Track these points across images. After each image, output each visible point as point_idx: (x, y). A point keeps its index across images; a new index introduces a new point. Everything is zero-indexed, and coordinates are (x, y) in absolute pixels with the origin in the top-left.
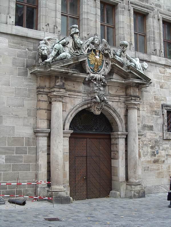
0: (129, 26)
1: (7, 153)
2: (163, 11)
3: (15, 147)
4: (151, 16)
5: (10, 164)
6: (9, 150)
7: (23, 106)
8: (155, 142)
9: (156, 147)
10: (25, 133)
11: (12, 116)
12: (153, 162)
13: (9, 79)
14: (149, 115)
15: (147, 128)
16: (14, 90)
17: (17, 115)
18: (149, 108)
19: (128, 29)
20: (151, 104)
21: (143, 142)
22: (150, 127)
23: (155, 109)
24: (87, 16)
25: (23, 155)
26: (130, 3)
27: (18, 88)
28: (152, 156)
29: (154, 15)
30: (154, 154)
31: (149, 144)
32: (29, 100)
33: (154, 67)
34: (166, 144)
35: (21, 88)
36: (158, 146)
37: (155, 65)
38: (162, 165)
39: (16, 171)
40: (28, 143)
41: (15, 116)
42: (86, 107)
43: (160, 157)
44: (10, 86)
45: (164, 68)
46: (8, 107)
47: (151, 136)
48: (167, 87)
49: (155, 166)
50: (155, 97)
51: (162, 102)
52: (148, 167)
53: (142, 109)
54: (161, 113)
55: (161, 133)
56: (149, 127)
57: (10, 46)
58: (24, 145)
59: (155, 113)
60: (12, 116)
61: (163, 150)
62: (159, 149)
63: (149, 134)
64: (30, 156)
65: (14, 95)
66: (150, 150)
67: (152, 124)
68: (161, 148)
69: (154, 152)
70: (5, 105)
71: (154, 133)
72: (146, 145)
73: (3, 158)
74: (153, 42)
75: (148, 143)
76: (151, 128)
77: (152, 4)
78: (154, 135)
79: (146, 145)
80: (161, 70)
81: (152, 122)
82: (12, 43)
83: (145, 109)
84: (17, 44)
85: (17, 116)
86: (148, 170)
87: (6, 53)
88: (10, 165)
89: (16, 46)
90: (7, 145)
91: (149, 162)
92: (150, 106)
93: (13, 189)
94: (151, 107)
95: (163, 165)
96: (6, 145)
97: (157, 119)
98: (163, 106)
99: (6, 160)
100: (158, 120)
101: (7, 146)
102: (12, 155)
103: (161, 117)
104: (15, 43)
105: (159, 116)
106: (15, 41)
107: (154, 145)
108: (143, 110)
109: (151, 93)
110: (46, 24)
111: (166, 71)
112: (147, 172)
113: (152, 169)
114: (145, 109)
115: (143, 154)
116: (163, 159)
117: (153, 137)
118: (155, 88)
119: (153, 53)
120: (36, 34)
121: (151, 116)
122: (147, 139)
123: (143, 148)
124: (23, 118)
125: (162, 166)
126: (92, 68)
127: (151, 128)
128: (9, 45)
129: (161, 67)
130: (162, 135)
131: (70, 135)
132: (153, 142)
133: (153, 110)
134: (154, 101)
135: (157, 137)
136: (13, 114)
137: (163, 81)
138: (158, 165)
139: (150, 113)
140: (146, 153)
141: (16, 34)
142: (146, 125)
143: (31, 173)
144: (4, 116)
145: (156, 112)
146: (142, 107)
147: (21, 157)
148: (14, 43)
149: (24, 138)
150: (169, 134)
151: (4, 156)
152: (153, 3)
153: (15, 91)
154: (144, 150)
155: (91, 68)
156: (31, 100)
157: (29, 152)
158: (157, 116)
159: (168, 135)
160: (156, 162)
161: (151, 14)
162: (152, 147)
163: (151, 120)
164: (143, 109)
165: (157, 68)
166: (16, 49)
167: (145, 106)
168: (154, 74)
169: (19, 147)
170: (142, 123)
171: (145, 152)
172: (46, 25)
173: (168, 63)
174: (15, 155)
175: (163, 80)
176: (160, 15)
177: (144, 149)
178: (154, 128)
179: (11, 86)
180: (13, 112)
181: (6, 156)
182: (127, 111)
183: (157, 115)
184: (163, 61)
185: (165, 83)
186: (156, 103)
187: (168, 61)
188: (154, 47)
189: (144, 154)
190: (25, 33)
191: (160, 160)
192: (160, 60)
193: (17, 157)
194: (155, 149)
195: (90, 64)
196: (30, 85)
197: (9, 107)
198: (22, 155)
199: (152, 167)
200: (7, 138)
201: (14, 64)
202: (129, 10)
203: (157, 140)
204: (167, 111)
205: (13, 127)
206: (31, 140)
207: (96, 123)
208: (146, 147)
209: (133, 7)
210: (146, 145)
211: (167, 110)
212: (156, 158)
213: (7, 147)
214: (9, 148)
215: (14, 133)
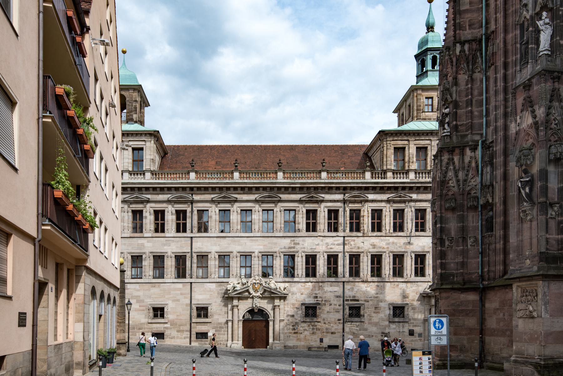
49: (295, 335)
66: (291, 327)
85: (220, 314)
91: (290, 333)
95: (301, 335)
109: (291, 299)
135: (297, 321)
160: (295, 333)
162: (293, 326)
176: (303, 254)
184: (304, 280)
201: (218, 294)
212: (296, 331)
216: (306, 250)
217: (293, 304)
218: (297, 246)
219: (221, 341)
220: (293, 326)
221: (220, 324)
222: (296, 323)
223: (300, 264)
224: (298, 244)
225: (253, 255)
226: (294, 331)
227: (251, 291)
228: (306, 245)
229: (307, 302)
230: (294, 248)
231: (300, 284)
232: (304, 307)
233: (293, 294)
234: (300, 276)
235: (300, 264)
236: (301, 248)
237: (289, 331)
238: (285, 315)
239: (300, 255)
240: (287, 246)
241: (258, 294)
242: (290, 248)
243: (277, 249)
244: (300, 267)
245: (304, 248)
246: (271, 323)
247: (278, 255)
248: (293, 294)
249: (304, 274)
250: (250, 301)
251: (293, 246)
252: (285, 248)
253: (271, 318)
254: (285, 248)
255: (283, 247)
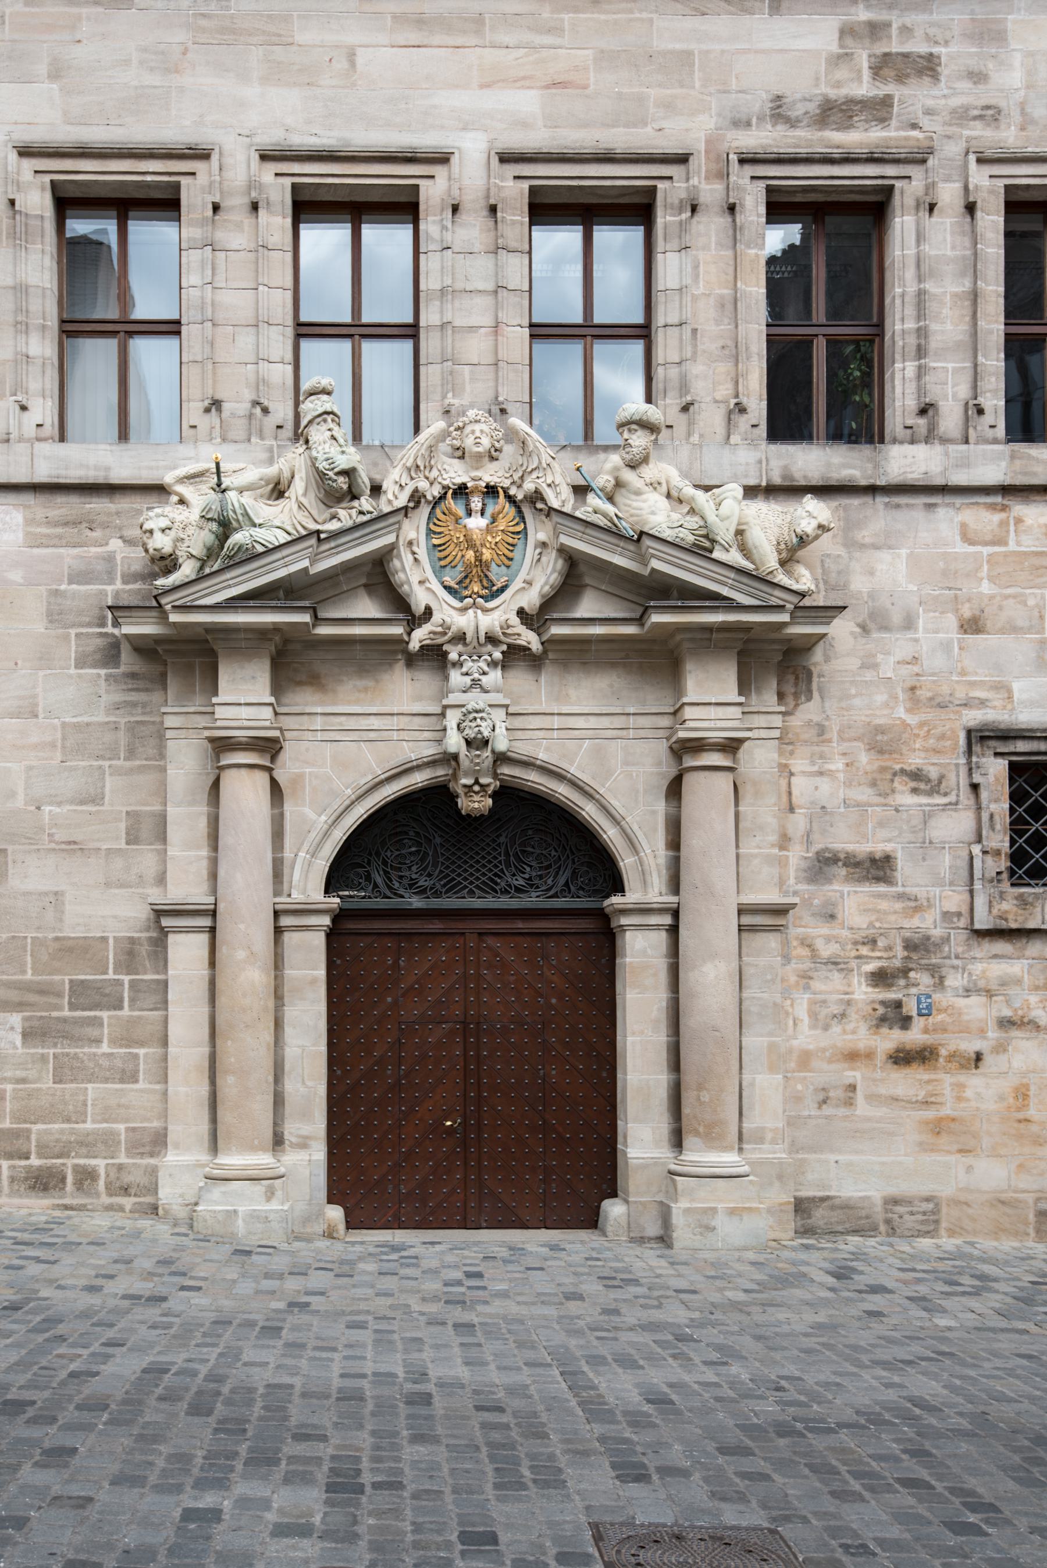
0: (729, 307)
1: (30, 1005)
2: (1019, 144)
3: (67, 978)
4: (909, 201)
5: (43, 1055)
6: (42, 992)
7: (97, 799)
8: (910, 946)
9: (912, 974)
10: (115, 917)
11: (53, 845)
12: (891, 1057)
13: (34, 687)
14: (864, 794)
15: (843, 872)
16: (59, 735)
17: (75, 843)
18: (864, 759)
19: (718, 323)
20: (880, 730)
21: (809, 946)
22: (867, 864)
23: (915, 761)
24: (442, 312)
25: (105, 1015)
26: (742, 161)
27: (77, 727)
28: (878, 1026)
29: (930, 187)
30: (895, 1016)
31: (858, 957)
32: (130, 771)
33: (919, 515)
34: (995, 956)
35: (88, 724)
36: (933, 970)
37: (921, 500)
38: (962, 1078)
39: (72, 1081)
40: (129, 958)
41: (63, 846)
42: (418, 779)
43: (945, 1030)
44: (36, 716)
45: (1004, 508)
46: (33, 808)
47: (878, 911)
48: (1020, 623)
49: (905, 1082)
50: (913, 689)
51: (974, 717)
52: (852, 1088)
53: (813, 763)
54: (964, 782)
55: (959, 893)
56: (857, 864)
57: (34, 542)
58: (111, 971)
59: (913, 784)
60: (53, 845)
61: (968, 992)
62: (940, 983)
63: (856, 903)
64: (140, 1017)
65: (59, 756)
66: (864, 993)
67: (888, 847)
68: (955, 981)
69: (898, 1005)
70: (20, 802)
71: (901, 896)
72: (836, 963)
73: (12, 1028)
74: (911, 368)
75: (854, 953)
76: (878, 868)
77: (925, 122)
78: (898, 906)
79: (834, 962)
80: (972, 525)
81: (883, 833)
82: (39, 525)
83: (838, 764)
84: (66, 524)
85: (73, 847)
86: (849, 1103)
87: (16, 576)
88: (44, 1058)
89: (60, 537)
90: (30, 972)
91: (852, 1057)
92: (878, 749)
93: (58, 1157)
94: (881, 752)
95: (975, 1082)
96: (24, 972)
97: (927, 818)
98: (980, 737)
99: (26, 1035)
100: (932, 823)
101: (29, 976)
102: (55, 1014)
103: (957, 804)
104: (56, 524)
105: (946, 794)
106: (56, 512)
107: (897, 963)
108: (821, 773)
109: (860, 677)
110: (206, 403)
111: (1019, 521)
112: (842, 1111)
113: (880, 1096)
114: (832, 767)
115: (813, 1015)
116: (969, 1046)
117: (893, 918)
118: (916, 640)
119: (909, 431)
120: (153, 464)
121: (882, 800)
122: (845, 933)
123: (811, 982)
124: (103, 853)
125: (961, 1086)
126: (453, 584)
127: (878, 868)
128: (27, 534)
129: (977, 503)
130: (965, 909)
131: (326, 921)
132: (889, 948)
133: (897, 767)
134: (909, 711)
135: (928, 923)
136: (57, 838)
137: (986, 588)
138: (926, 1077)
139: (873, 784)
140: (836, 1009)
141: (56, 480)
142: (842, 856)
143: (142, 1091)
144: (17, 847)
145: (916, 775)
146: (813, 755)
147: (97, 1022)
148: (49, 523)
149: (111, 941)
150: (1020, 897)
151: (16, 1019)
152: (929, 112)
153: (64, 738)
154: (820, 993)
155: (445, 587)
156: (141, 769)
157: (132, 1000)
158: (924, 800)
159: (1005, 906)
160: (903, 1058)
161: (908, 191)
162: (881, 978)
163: (881, 824)
164: (816, 768)
165: (942, 512)
166: (62, 550)
167: (836, 746)
168: (910, 556)
169: (82, 981)
170: (809, 842)
171: (824, 1002)
172: (207, 410)
173: (1025, 474)
174: (66, 1013)
175: (991, 579)
176: (980, 177)
177: (817, 985)
178: (903, 867)
179: (41, 716)
180: (54, 831)
181: (25, 1019)
182: (675, 789)
183: (930, 793)
184: (993, 462)
185: (1007, 597)
186: (922, 724)
187: (1030, 457)
188: (921, 391)
189: (821, 1016)
190: (96, 468)
191: (943, 1052)
192: (964, 463)
193: (76, 1021)
194: (907, 986)
195: (443, 563)
196: (134, 705)
197: (38, 808)
198: (97, 1013)
199: (883, 1090)
200: (29, 941)
201: (54, 617)
202: (732, 209)
203: (928, 938)
204: (1012, 765)
205: (56, 893)
206: (144, 950)
207: (516, 855)
208: (836, 975)
209: (762, 184)
210: (834, 962)
211: (1014, 758)
212: (915, 1036)
213: (31, 981)
214: (39, 983)
215: (61, 920)
216: (1009, 137)
217: (882, 741)
218: (914, 97)
219: (87, 1144)
220: (881, 978)
221: (79, 950)
222: (918, 946)
223: (945, 290)
224: (928, 67)
225: (433, 192)
226: (892, 1038)
227: (420, 580)
228: (1010, 80)
229: (1026, 717)
230: (879, 109)
231: (947, 520)
232: (995, 770)
233: (875, 623)
234: (950, 418)
235: (945, 290)
236: (962, 116)
237: (838, 1037)
238: (796, 856)
239: (949, 194)
240: (806, 87)
241: (498, 616)
242: (834, 112)
243: (689, 129)
244: (948, 326)
245: (991, 115)
246: (640, 950)
247: (711, 192)
248: (875, 623)
249: (995, 402)
250: (404, 691)
251: (864, 88)
252: (779, 111)
253: (644, 883)
254: (779, 111)
255: (758, 103)
